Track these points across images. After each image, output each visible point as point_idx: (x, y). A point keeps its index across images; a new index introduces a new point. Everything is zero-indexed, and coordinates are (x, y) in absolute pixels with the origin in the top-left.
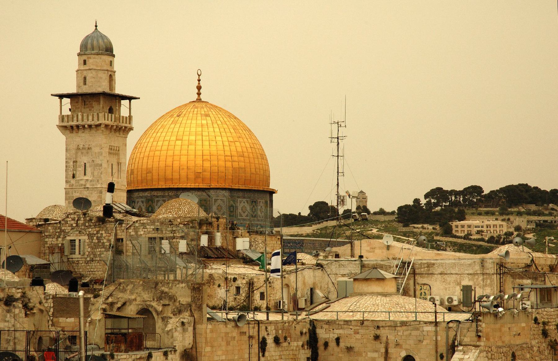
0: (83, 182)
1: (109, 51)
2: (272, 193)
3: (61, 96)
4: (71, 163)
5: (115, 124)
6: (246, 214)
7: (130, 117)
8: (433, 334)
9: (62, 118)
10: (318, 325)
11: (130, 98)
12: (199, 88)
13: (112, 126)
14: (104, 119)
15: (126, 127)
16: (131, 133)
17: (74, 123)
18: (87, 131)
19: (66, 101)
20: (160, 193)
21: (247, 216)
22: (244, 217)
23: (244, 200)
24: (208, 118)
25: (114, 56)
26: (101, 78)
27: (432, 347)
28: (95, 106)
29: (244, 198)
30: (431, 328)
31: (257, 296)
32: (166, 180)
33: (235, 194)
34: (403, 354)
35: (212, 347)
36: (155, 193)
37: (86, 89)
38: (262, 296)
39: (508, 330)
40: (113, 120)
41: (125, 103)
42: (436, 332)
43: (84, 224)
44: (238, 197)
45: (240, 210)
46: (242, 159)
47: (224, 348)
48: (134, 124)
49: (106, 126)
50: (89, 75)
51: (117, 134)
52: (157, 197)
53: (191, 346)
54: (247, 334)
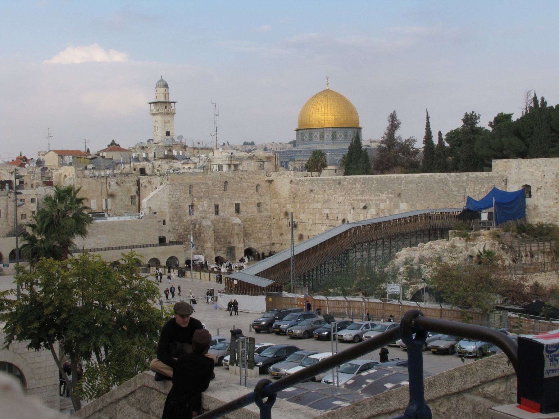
1: (166, 86)
2: (360, 128)
3: (150, 103)
7: (175, 110)
11: (174, 102)
12: (328, 84)
14: (164, 111)
16: (175, 115)
19: (152, 104)
20: (305, 131)
28: (164, 106)
30: (159, 178)
31: (156, 170)
33: (336, 130)
37: (157, 101)
38: (158, 170)
41: (173, 104)
45: (338, 136)
48: (176, 111)
49: (162, 113)
50: (158, 95)
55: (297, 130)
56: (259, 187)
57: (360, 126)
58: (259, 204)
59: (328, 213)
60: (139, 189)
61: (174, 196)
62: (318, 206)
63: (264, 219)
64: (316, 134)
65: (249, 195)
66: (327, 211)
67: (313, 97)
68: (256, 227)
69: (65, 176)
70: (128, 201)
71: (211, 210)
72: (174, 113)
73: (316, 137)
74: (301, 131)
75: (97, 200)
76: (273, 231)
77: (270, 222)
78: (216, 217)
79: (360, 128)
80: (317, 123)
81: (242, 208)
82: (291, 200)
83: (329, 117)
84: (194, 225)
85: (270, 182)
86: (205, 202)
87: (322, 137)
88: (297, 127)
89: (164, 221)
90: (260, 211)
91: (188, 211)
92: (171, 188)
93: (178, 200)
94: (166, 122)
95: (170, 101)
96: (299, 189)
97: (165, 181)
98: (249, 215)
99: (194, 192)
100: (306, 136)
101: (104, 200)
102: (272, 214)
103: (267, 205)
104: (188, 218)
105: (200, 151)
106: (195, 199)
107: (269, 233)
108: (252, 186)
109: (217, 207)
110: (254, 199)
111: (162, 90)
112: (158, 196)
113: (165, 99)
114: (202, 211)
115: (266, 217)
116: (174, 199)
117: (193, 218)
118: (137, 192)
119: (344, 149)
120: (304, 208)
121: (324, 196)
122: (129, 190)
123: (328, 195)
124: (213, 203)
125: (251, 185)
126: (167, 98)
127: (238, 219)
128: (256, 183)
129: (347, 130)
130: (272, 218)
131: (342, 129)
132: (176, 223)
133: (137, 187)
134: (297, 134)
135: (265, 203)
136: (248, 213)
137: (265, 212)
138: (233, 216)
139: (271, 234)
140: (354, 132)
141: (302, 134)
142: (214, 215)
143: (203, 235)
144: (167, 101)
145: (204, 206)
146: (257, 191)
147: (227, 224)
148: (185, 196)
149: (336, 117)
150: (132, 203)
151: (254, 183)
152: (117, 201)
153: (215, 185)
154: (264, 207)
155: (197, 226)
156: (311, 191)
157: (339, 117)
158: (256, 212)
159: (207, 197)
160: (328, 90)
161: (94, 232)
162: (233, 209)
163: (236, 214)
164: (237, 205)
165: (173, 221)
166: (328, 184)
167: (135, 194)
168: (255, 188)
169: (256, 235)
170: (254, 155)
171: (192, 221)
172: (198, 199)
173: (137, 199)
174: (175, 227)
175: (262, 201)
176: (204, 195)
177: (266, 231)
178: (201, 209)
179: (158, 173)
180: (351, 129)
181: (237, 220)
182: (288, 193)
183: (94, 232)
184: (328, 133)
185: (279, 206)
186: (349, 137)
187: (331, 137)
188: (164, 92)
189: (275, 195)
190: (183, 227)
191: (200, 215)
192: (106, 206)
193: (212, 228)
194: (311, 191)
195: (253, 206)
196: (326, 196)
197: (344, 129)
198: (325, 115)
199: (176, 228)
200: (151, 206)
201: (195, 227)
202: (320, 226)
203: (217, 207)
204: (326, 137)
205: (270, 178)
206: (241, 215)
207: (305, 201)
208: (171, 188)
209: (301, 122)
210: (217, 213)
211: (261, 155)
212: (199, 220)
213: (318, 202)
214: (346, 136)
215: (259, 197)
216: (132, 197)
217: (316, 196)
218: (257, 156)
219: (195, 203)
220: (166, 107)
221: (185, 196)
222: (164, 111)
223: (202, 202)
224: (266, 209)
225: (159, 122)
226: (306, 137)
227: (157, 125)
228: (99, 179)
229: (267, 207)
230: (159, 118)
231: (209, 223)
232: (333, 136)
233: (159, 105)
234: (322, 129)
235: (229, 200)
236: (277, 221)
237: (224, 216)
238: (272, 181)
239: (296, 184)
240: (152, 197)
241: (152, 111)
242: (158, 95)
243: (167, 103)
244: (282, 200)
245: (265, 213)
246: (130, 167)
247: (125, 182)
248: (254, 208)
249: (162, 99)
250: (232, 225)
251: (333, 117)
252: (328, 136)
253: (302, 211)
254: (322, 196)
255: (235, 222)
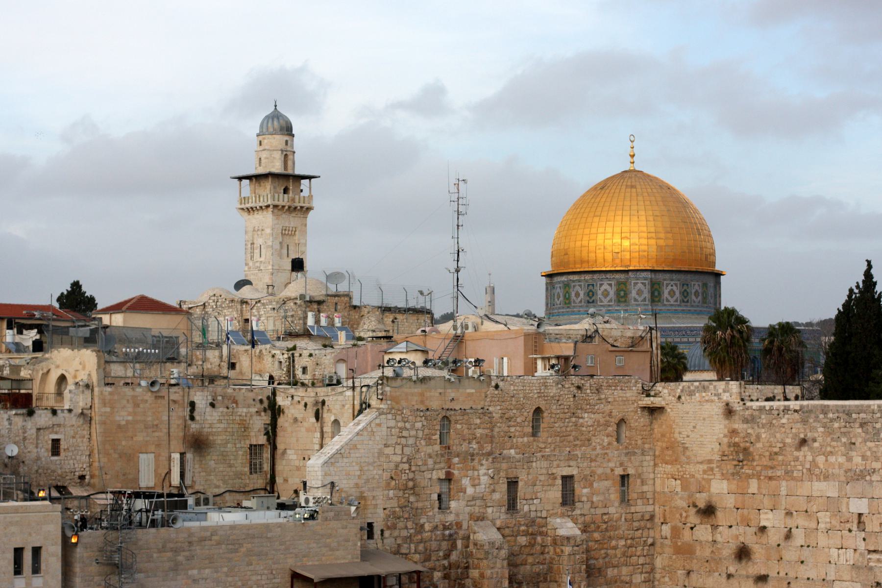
0: (258, 264)
1: (288, 130)
2: (718, 275)
3: (240, 179)
4: (249, 246)
5: (288, 204)
6: (675, 298)
8: (351, 398)
9: (244, 200)
10: (278, 393)
11: (310, 178)
12: (633, 156)
13: (283, 207)
15: (302, 207)
16: (311, 212)
17: (249, 206)
18: (260, 212)
20: (576, 277)
21: (676, 301)
22: (672, 303)
23: (672, 283)
24: (634, 190)
25: (293, 136)
26: (274, 158)
27: (351, 411)
29: (672, 280)
30: (349, 393)
32: (582, 262)
33: (660, 276)
34: (333, 419)
35: (112, 408)
36: (571, 277)
37: (261, 171)
38: (304, 370)
39: (438, 395)
40: (286, 200)
42: (354, 396)
43: (221, 306)
44: (665, 280)
45: (666, 294)
46: (670, 235)
47: (130, 410)
48: (315, 203)
49: (275, 206)
50: (264, 155)
51: (293, 214)
52: (574, 281)
53: (88, 406)
54: (166, 398)
55: (550, 276)
56: (624, 428)
57: (718, 268)
58: (624, 478)
59: (864, 510)
60: (274, 424)
61: (398, 450)
62: (829, 489)
63: (636, 524)
64: (606, 289)
65: (599, 450)
66: (859, 506)
67: (595, 188)
68: (615, 548)
69: (62, 379)
70: (241, 463)
71: (496, 496)
72: (309, 209)
73: (606, 294)
74: (564, 278)
75: (157, 458)
76: (659, 562)
77: (651, 533)
78: (509, 516)
79: (718, 275)
80: (609, 256)
81: (582, 491)
82: (729, 467)
83: (644, 241)
84: (452, 539)
85: (653, 411)
86: (482, 471)
87: (622, 297)
88: (549, 269)
89: (370, 525)
90: (624, 500)
91: (435, 497)
92: (392, 423)
93: (409, 462)
94: (287, 233)
95: (298, 172)
96: (758, 437)
97: (374, 402)
98: (599, 511)
99: (453, 440)
100: (579, 291)
101: (176, 456)
102: (658, 511)
103: (643, 483)
104: (439, 518)
105: (400, 317)
106: (456, 460)
107: (647, 568)
108: (607, 425)
109: (513, 484)
110: (612, 465)
111: (278, 140)
112: (355, 447)
113: (286, 168)
114: (474, 499)
115: (642, 519)
116: (398, 459)
117: (451, 518)
118: (267, 434)
119: (691, 329)
120: (775, 495)
121: (850, 459)
122: (245, 427)
123: (864, 457)
124: (502, 474)
125: (602, 421)
126: (290, 163)
127: (571, 524)
128: (617, 415)
129: (689, 277)
130: (658, 520)
131: (675, 276)
132: (405, 533)
133: (266, 418)
134: (550, 287)
135: (639, 476)
136: (593, 506)
137: (639, 502)
138: (555, 515)
139: (653, 570)
140: (705, 285)
141: (567, 285)
142: (504, 509)
143: (474, 573)
144: (290, 172)
145: (479, 482)
146: (618, 440)
147: (539, 539)
148: (429, 449)
149: (662, 242)
150: (254, 468)
151: (610, 415)
152: (212, 461)
153: (509, 419)
154: (635, 487)
155: (459, 543)
156: (803, 442)
157: (671, 242)
158: (617, 504)
159: (489, 454)
160: (634, 171)
161: (180, 558)
162: (555, 493)
163: (564, 509)
164: (567, 480)
165: (394, 527)
166: (862, 425)
167: (262, 440)
168: (611, 429)
169: (616, 571)
170: (597, 331)
171: (445, 528)
172: (464, 461)
173: (267, 455)
174: (399, 546)
175: (631, 471)
176: (481, 447)
177: (641, 560)
178: (470, 491)
179: (307, 378)
180: (697, 277)
181: (567, 528)
182: (716, 447)
183: (180, 558)
184: (640, 286)
185: (684, 488)
186: (693, 297)
187: (646, 294)
188: (283, 146)
189: (675, 452)
190: (421, 547)
191: (468, 509)
192: (182, 475)
193: (504, 553)
194: (803, 442)
195: (607, 483)
196: (858, 460)
197: (682, 277)
198: (623, 239)
199: (404, 551)
200: (335, 479)
201: (454, 546)
202: (834, 552)
203: (513, 484)
204: (634, 294)
205: (657, 402)
206: (578, 512)
207: (779, 473)
208: (392, 423)
209: (560, 254)
210: (512, 505)
211: (616, 333)
212: (465, 526)
213: (826, 478)
214: (685, 294)
215: (626, 459)
216: (254, 450)
217: (821, 459)
218: (605, 334)
219: (456, 472)
220: (286, 191)
221: (429, 449)
222: (283, 200)
223: (474, 469)
224: (642, 496)
225: (268, 231)
226: (577, 295)
227: (259, 241)
228: (164, 391)
229: (645, 488)
230: (266, 219)
231: (496, 536)
232: (652, 294)
233: (268, 185)
234: (622, 276)
235: (545, 464)
236: (676, 532)
237: (533, 515)
238: (661, 409)
239: (746, 421)
240: (339, 453)
241: (244, 200)
242: (264, 155)
243: (288, 180)
244: (696, 470)
245: (640, 507)
246: (221, 357)
247: (236, 402)
248: (612, 490)
249: (277, 167)
250: (554, 543)
251: (653, 242)
252: (640, 292)
253: (767, 502)
254: (842, 459)
255: (562, 532)
